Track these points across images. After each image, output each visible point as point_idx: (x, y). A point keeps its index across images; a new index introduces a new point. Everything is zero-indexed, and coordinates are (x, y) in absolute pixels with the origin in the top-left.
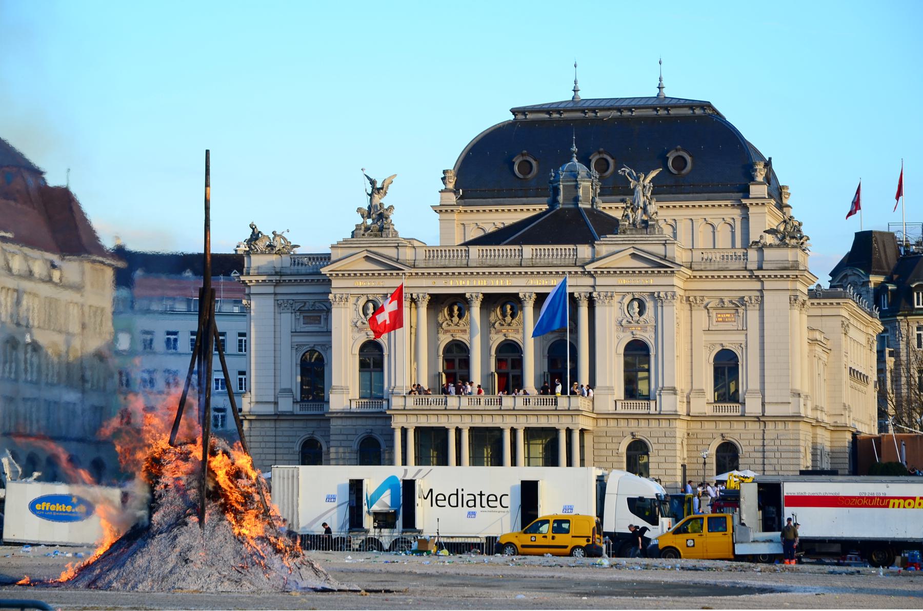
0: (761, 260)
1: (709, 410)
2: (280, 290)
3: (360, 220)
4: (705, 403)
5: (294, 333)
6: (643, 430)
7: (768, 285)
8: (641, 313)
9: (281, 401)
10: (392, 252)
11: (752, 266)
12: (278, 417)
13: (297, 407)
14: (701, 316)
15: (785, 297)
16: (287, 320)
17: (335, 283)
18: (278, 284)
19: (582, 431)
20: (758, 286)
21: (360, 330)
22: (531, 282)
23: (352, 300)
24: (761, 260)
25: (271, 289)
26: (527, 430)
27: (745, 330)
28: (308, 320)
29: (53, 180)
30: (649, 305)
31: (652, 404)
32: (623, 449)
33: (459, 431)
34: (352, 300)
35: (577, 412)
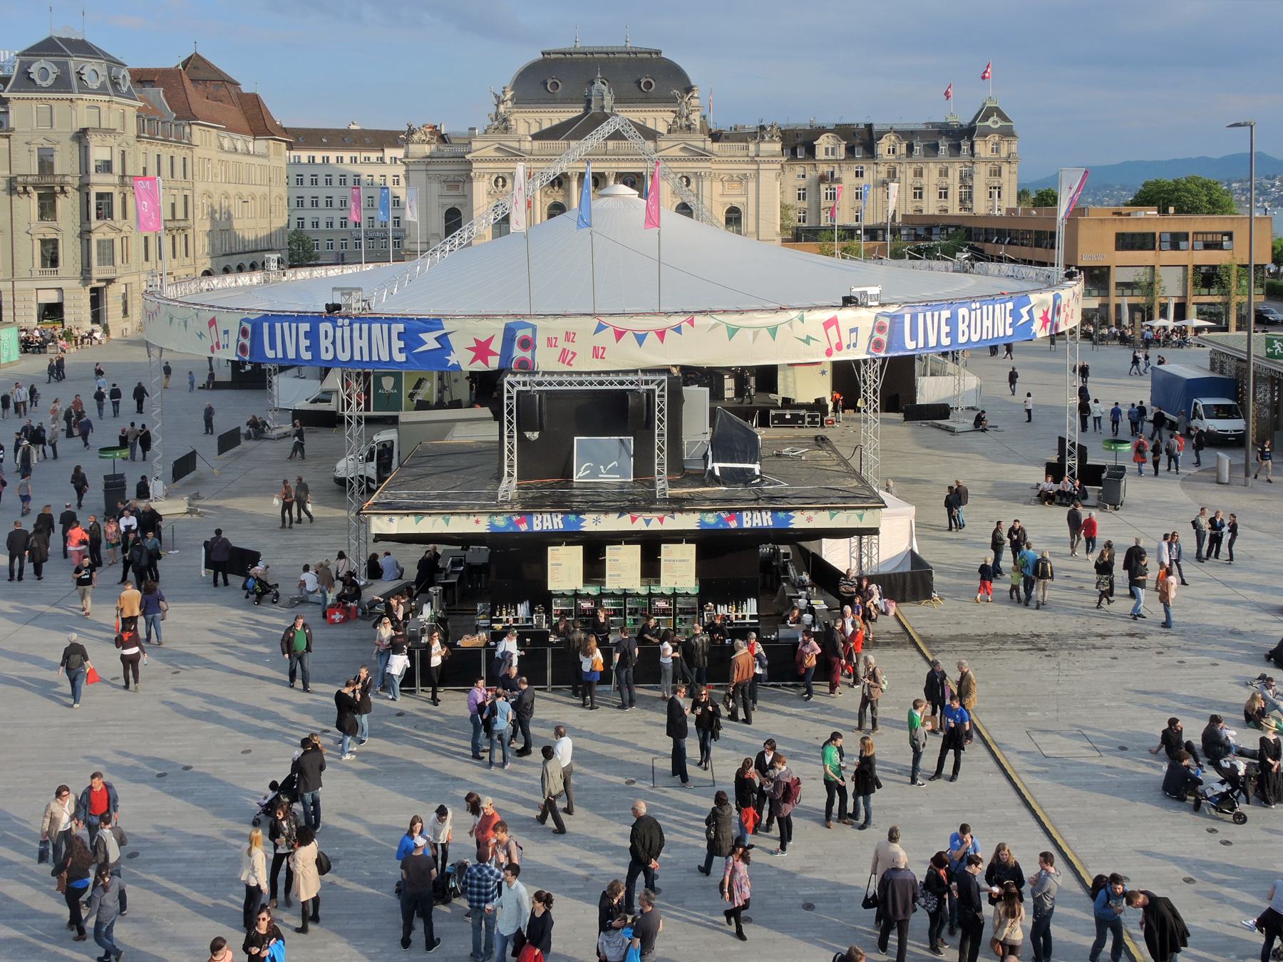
0: (758, 150)
7: (762, 166)
10: (516, 145)
11: (752, 154)
14: (718, 186)
16: (436, 188)
17: (475, 165)
18: (429, 163)
20: (755, 167)
23: (487, 176)
24: (758, 150)
25: (424, 167)
28: (450, 187)
29: (246, 89)
30: (693, 181)
34: (487, 176)
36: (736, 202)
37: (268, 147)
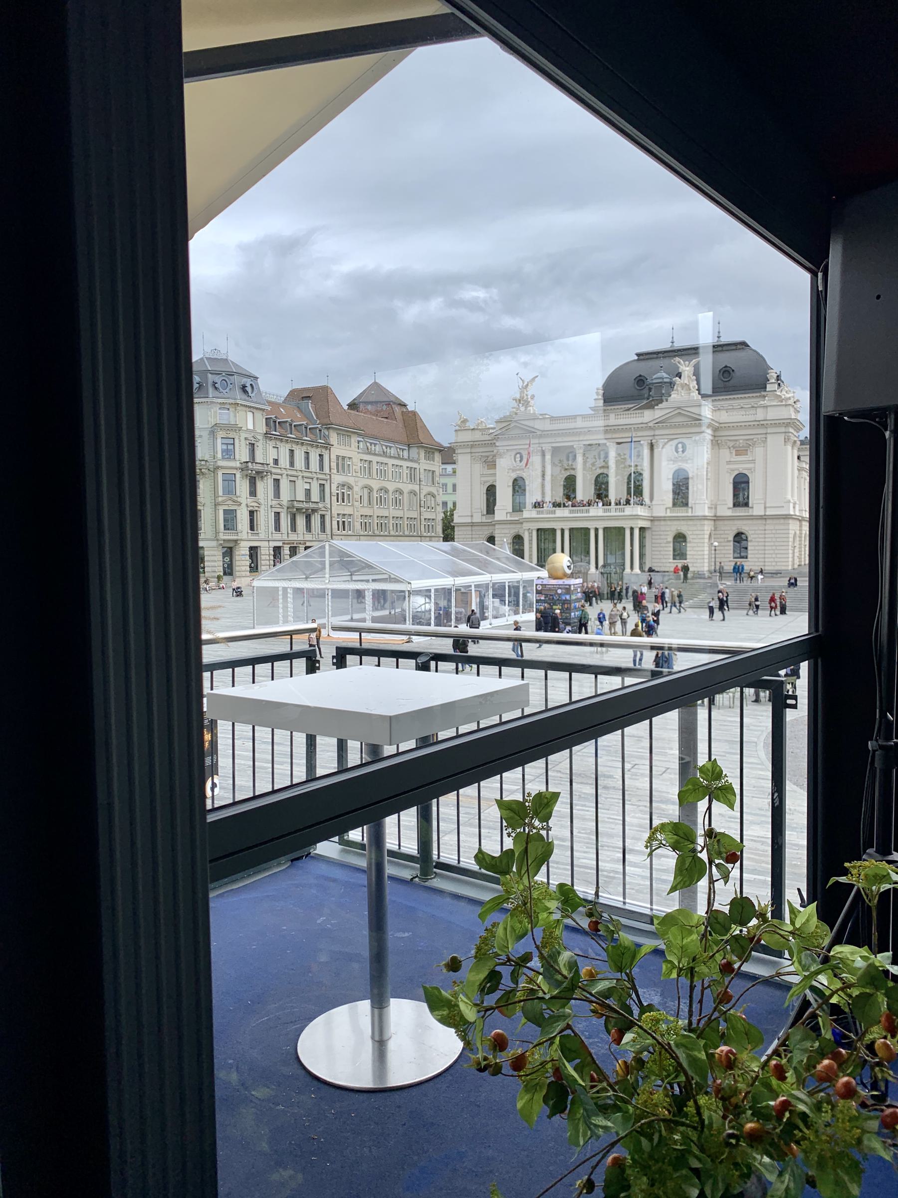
1: (729, 513)
2: (473, 450)
3: (515, 404)
4: (726, 507)
5: (482, 475)
6: (684, 528)
8: (683, 452)
9: (474, 515)
12: (472, 525)
13: (484, 517)
15: (781, 438)
16: (478, 468)
18: (472, 446)
19: (642, 529)
21: (513, 471)
22: (614, 436)
25: (469, 450)
26: (605, 529)
27: (753, 461)
31: (690, 510)
32: (670, 539)
33: (563, 530)
35: (637, 517)
36: (742, 468)
37: (419, 453)
